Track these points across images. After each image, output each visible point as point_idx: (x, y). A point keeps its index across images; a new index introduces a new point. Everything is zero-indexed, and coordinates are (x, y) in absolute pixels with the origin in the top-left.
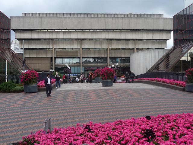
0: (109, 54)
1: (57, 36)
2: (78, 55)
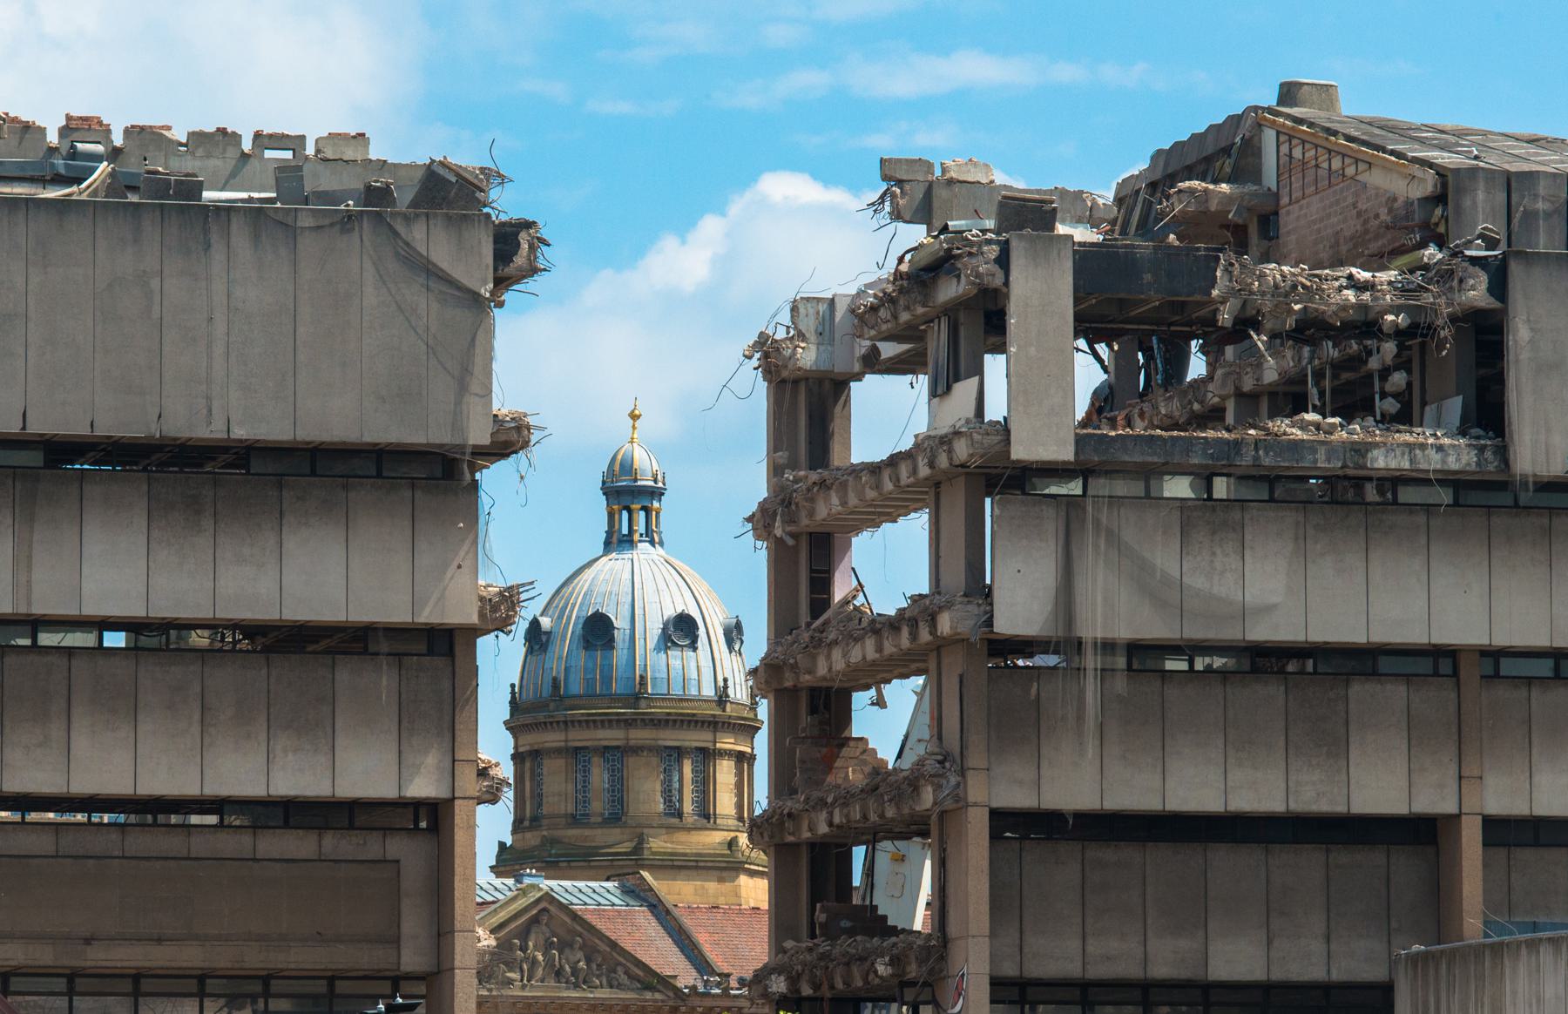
0: (993, 934)
1: (23, 561)
2: (396, 941)
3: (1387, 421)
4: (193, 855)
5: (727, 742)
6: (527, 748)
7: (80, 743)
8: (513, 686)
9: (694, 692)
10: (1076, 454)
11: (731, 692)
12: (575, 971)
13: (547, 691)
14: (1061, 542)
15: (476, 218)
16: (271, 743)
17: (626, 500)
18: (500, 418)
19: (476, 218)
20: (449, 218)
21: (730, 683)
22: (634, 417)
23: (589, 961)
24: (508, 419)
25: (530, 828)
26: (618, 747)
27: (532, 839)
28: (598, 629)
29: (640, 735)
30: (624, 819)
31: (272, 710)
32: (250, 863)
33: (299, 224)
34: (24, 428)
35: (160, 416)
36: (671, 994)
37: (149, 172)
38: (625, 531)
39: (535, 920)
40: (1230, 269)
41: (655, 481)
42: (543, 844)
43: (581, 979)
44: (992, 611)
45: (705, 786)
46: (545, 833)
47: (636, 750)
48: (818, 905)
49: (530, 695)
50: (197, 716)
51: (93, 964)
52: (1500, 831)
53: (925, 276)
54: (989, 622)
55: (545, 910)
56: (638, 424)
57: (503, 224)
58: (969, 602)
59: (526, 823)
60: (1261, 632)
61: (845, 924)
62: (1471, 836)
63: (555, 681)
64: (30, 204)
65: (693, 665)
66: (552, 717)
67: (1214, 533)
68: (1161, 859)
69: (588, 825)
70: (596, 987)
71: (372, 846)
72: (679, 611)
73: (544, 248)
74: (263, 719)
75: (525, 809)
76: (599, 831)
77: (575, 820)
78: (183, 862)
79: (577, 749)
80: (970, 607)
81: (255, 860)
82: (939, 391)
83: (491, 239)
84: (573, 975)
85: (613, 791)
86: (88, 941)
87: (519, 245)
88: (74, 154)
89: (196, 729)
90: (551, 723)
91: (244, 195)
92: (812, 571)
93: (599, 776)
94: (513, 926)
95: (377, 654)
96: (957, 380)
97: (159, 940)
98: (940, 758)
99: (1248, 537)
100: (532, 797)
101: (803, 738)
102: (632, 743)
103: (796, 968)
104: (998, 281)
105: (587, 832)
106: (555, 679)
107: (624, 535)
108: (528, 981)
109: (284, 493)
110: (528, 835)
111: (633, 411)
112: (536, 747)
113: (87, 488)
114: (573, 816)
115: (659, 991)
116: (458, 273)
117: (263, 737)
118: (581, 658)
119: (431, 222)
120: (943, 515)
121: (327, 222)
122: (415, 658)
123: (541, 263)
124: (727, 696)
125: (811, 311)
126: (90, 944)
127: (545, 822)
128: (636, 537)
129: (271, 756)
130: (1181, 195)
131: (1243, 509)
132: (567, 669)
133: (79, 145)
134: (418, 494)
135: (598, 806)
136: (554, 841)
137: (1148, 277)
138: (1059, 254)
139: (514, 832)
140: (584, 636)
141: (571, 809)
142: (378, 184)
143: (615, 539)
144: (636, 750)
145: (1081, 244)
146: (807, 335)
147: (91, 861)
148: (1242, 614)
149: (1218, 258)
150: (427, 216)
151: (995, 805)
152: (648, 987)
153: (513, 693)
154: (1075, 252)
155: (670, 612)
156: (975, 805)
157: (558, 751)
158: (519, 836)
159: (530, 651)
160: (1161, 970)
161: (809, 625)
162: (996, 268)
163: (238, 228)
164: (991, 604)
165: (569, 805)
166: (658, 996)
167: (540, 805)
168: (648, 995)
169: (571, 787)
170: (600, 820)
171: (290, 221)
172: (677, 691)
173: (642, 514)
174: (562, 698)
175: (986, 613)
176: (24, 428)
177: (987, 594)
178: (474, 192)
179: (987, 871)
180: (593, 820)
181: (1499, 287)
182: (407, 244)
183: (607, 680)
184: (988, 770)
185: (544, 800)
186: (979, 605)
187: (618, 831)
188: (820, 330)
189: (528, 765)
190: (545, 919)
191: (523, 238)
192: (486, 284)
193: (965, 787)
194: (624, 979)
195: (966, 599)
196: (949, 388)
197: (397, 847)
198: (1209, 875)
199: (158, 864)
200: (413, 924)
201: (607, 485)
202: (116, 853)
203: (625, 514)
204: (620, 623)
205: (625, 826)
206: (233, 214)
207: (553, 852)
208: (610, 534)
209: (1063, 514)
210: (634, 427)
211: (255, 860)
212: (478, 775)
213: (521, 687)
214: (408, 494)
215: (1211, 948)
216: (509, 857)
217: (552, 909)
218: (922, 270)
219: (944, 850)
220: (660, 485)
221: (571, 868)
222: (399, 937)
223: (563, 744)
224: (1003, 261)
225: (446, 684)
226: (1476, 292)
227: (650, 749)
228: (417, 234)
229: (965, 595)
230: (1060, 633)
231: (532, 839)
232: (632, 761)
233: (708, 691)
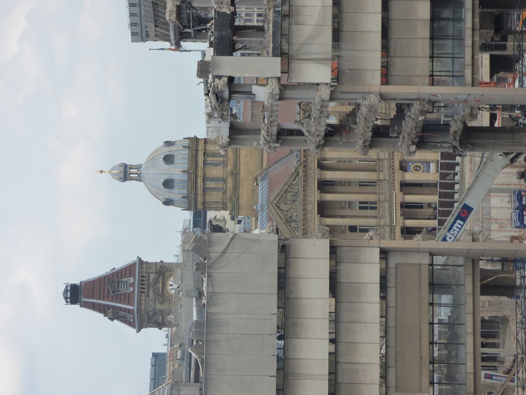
0: (416, 85)
2: (420, 265)
4: (395, 326)
5: (201, 147)
6: (202, 206)
7: (364, 360)
8: (182, 210)
9: (187, 156)
10: (278, 56)
11: (187, 145)
12: (294, 196)
13: (186, 200)
14: (305, 62)
15: (209, 238)
16: (364, 302)
17: (127, 174)
18: (269, 231)
19: (209, 238)
20: (209, 246)
21: (184, 145)
22: (102, 172)
23: (290, 192)
24: (270, 229)
25: (226, 206)
26: (203, 179)
27: (229, 205)
28: (168, 184)
29: (200, 173)
30: (225, 178)
31: (354, 302)
32: (397, 308)
33: (211, 292)
34: (275, 376)
35: (271, 335)
36: (300, 167)
37: (192, 337)
38: (137, 175)
39: (278, 207)
40: (221, 8)
41: (122, 166)
42: (231, 202)
43: (296, 194)
44: (324, 83)
45: (215, 155)
46: (228, 201)
47: (204, 174)
48: (390, 135)
49: (186, 206)
50: (356, 324)
51: (428, 357)
53: (220, 100)
54: (327, 84)
55: (275, 204)
56: (104, 171)
57: (211, 230)
58: (321, 90)
59: (224, 207)
61: (396, 127)
63: (182, 197)
64: (207, 374)
65: (179, 156)
66: (193, 199)
67: (299, 15)
68: (395, 32)
69: (226, 189)
70: (298, 190)
71: (392, 272)
72: (162, 160)
73: (217, 217)
74: (357, 304)
75: (219, 207)
76: (228, 185)
77: (225, 193)
78: (397, 329)
79: (203, 191)
80: (322, 90)
81: (396, 307)
82: (254, 97)
83: (215, 233)
84: (295, 197)
85: (216, 181)
86: (421, 358)
87: (217, 225)
88: (182, 359)
89: (359, 325)
90: (195, 199)
91: (195, 308)
92: (288, 135)
93: (210, 184)
94: (280, 214)
95: (336, 270)
96: (251, 92)
97: (421, 336)
98: (364, 99)
99: (301, 4)
100: (216, 205)
101: (340, 139)
102: (202, 175)
103: (410, 143)
104: (226, 79)
105: (228, 189)
106: (182, 197)
107: (138, 176)
108: (297, 210)
109: (290, 297)
110: (228, 206)
111: (100, 172)
112: (202, 203)
113: (290, 357)
114: (223, 193)
115: (299, 171)
116: (226, 244)
117: (362, 304)
118: (176, 190)
119: (210, 251)
120: (290, 97)
121: (210, 283)
122: (337, 258)
123: (222, 218)
124: (188, 146)
125: (211, 134)
126: (422, 358)
127: (224, 201)
128: (139, 172)
129: (367, 302)
130: (171, 19)
131: (292, 6)
132: (179, 194)
133: (178, 358)
134: (290, 256)
135: (220, 185)
136: (231, 199)
137: (224, 33)
138: (218, 60)
139: (226, 210)
140: (170, 189)
141: (221, 193)
142: (195, 267)
143: (139, 179)
144: (204, 174)
145: (214, 53)
146: (218, 135)
147: (397, 357)
149: (218, 11)
150: (208, 253)
151: (380, 83)
152: (298, 174)
153: (185, 210)
154: (217, 55)
155: (161, 162)
156: (380, 89)
157: (204, 197)
158: (228, 209)
159: (173, 204)
160: (427, 34)
161: (306, 137)
162: (222, 80)
163: (212, 310)
164: (321, 83)
165: (220, 194)
166: (300, 172)
167: (219, 202)
168: (300, 174)
169: (215, 193)
170: (225, 185)
171: (211, 294)
172: (187, 161)
173: (131, 170)
174: (188, 195)
175: (324, 85)
176: (275, 376)
177: (318, 84)
178: (198, 238)
179: (400, 87)
180: (225, 187)
182: (217, 259)
183: (183, 181)
184: (369, 85)
185: (218, 201)
186: (322, 87)
187: (228, 180)
188: (217, 131)
189: (207, 206)
190: (278, 205)
191: (214, 223)
192: (229, 235)
193: (375, 92)
194: (295, 181)
195: (319, 91)
196: (254, 95)
197: (392, 263)
198: (398, 19)
199: (398, 336)
200: (415, 259)
201: (123, 180)
202: (395, 349)
203: (131, 175)
204: (166, 177)
205: (227, 178)
206: (208, 312)
207: (234, 199)
208: (137, 180)
209: (294, 61)
210: (105, 172)
211: (396, 307)
212: (372, 239)
213: (183, 207)
214: (290, 259)
215: (420, 18)
216: (234, 212)
217: (275, 202)
218: (218, 102)
219: (391, 99)
220: (123, 165)
221: (239, 194)
222: (419, 264)
223: (202, 196)
224: (220, 77)
225: (345, 248)
227: (204, 170)
228: (214, 256)
229: (318, 91)
230: (330, 62)
231: (229, 205)
232: (208, 175)
233: (186, 151)
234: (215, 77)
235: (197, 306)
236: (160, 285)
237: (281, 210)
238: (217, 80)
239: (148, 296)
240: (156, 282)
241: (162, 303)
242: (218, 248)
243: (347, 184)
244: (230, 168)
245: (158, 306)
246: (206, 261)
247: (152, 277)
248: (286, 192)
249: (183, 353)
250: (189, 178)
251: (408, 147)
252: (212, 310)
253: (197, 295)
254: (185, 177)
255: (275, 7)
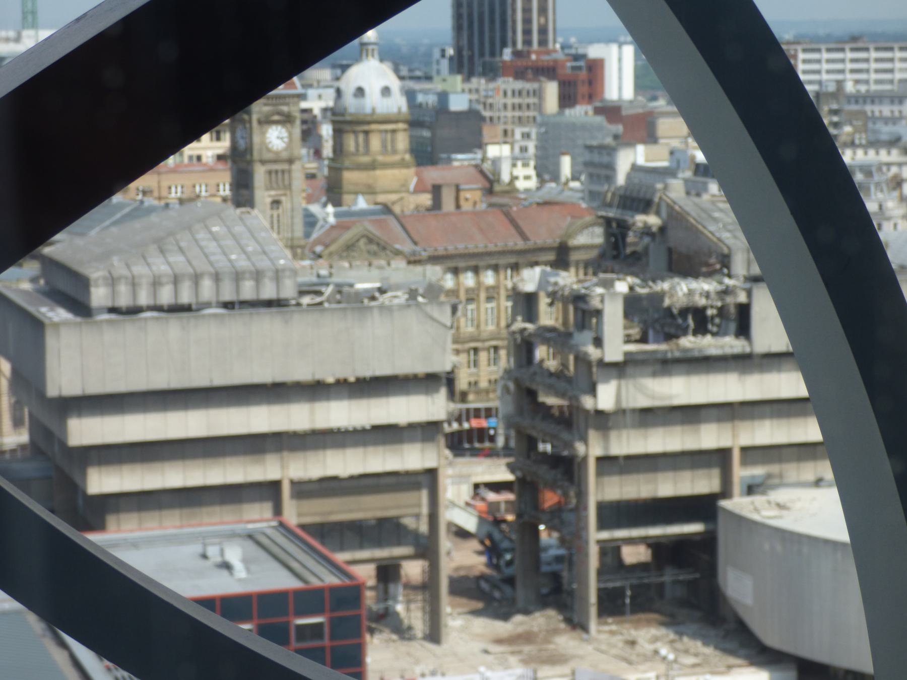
2: (419, 505)
3: (714, 334)
29: (374, 127)
52: (744, 450)
60: (677, 402)
62: (736, 456)
148: (671, 397)
163: (376, 313)
181: (749, 293)
224: (602, 301)
226: (742, 298)
228: (428, 309)
233: (395, 110)
234: (602, 297)
235: (373, 289)
236: (276, 118)
237: (358, 240)
238: (598, 299)
239: (266, 105)
240: (280, 113)
241: (260, 122)
242: (435, 311)
243: (483, 414)
244: (380, 158)
245: (255, 117)
246: (420, 299)
247: (285, 109)
248: (378, 244)
249: (324, 277)
250: (366, 115)
251: (521, 469)
252: (376, 313)
253: (384, 288)
254: (368, 110)
255: (672, 351)
